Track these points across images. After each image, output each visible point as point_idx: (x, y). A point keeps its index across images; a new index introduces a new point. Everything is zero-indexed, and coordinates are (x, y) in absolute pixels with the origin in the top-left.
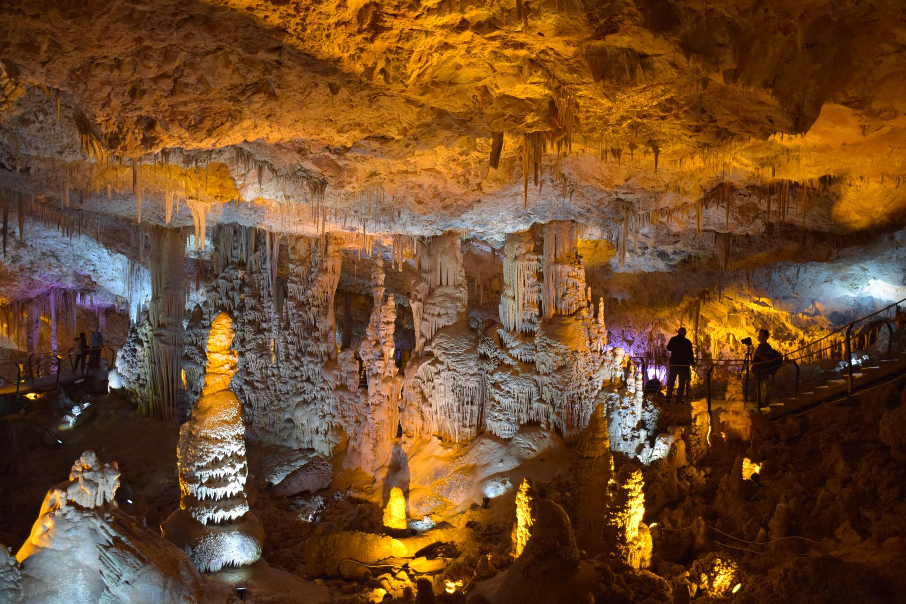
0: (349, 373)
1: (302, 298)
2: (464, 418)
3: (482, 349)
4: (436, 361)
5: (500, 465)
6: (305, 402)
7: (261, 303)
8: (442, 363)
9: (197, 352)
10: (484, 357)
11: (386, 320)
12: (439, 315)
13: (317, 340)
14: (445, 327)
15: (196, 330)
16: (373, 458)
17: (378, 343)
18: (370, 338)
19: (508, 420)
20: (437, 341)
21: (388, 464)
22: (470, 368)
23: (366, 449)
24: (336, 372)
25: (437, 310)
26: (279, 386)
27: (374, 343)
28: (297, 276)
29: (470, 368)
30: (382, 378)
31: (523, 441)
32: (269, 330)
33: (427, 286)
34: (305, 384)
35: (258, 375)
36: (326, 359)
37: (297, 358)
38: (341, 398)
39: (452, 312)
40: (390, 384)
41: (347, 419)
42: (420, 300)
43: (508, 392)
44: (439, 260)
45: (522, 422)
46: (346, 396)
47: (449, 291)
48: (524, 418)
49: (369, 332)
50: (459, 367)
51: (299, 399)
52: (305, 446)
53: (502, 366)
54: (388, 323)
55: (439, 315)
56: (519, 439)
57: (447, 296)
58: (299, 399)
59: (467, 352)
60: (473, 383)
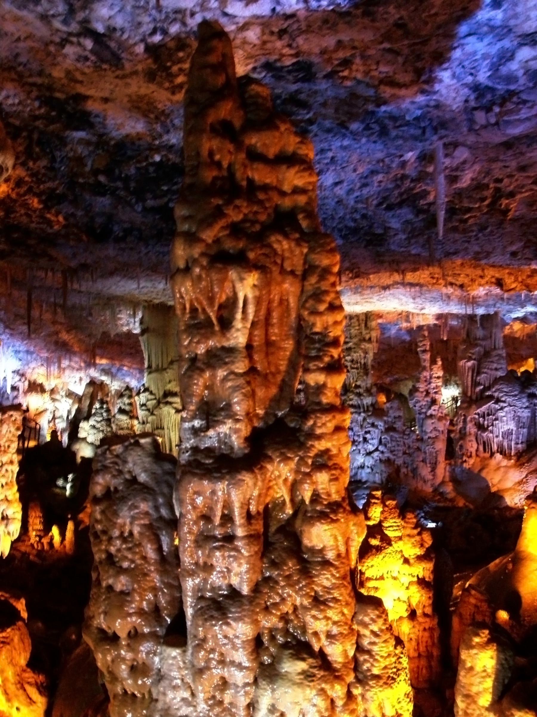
0: (395, 418)
4: (498, 401)
8: (504, 402)
11: (436, 375)
12: (496, 369)
13: (359, 395)
14: (501, 377)
16: (431, 477)
17: (428, 393)
18: (421, 390)
21: (447, 479)
23: (425, 471)
24: (385, 418)
25: (495, 366)
33: (482, 350)
36: (371, 409)
38: (391, 437)
40: (444, 422)
41: (396, 453)
42: (475, 359)
44: (494, 331)
47: (500, 352)
49: (422, 386)
50: (518, 404)
54: (438, 378)
55: (496, 369)
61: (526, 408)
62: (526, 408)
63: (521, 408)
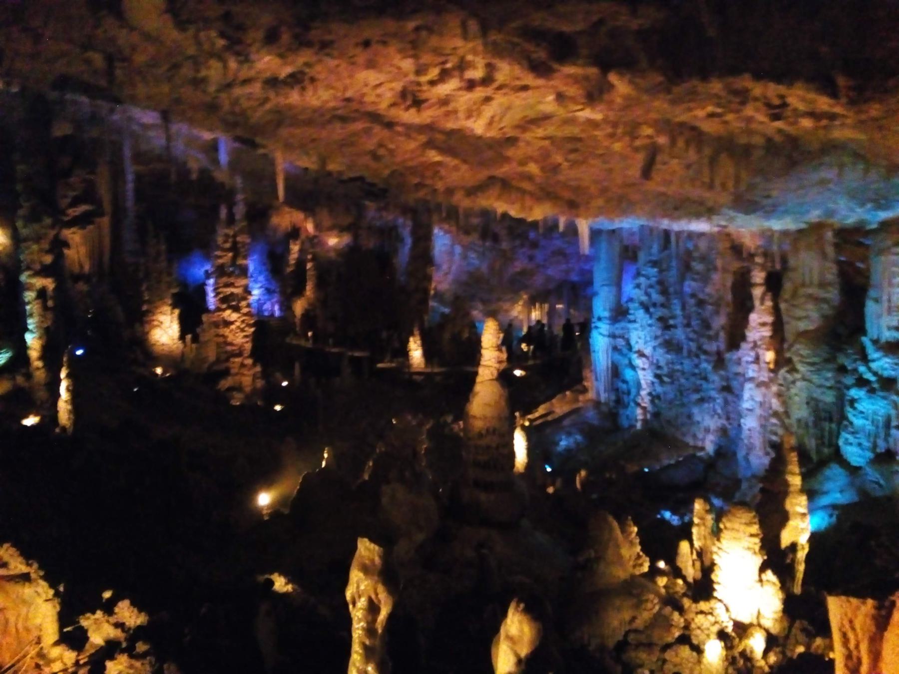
1: (701, 296)
2: (822, 437)
3: (843, 360)
5: (838, 495)
6: (702, 400)
7: (668, 299)
9: (623, 343)
10: (842, 370)
15: (623, 324)
19: (860, 445)
20: (797, 346)
22: (827, 379)
26: (683, 381)
27: (751, 345)
28: (698, 273)
29: (827, 379)
30: (756, 382)
31: (872, 474)
32: (675, 327)
34: (703, 382)
35: (665, 370)
37: (697, 356)
39: (815, 315)
43: (862, 412)
45: (878, 450)
46: (730, 398)
48: (882, 447)
51: (696, 397)
52: (700, 444)
53: (862, 382)
56: (869, 470)
57: (810, 297)
58: (696, 397)
59: (827, 361)
60: (829, 398)
61: (830, 388)
62: (830, 388)
63: (820, 386)
